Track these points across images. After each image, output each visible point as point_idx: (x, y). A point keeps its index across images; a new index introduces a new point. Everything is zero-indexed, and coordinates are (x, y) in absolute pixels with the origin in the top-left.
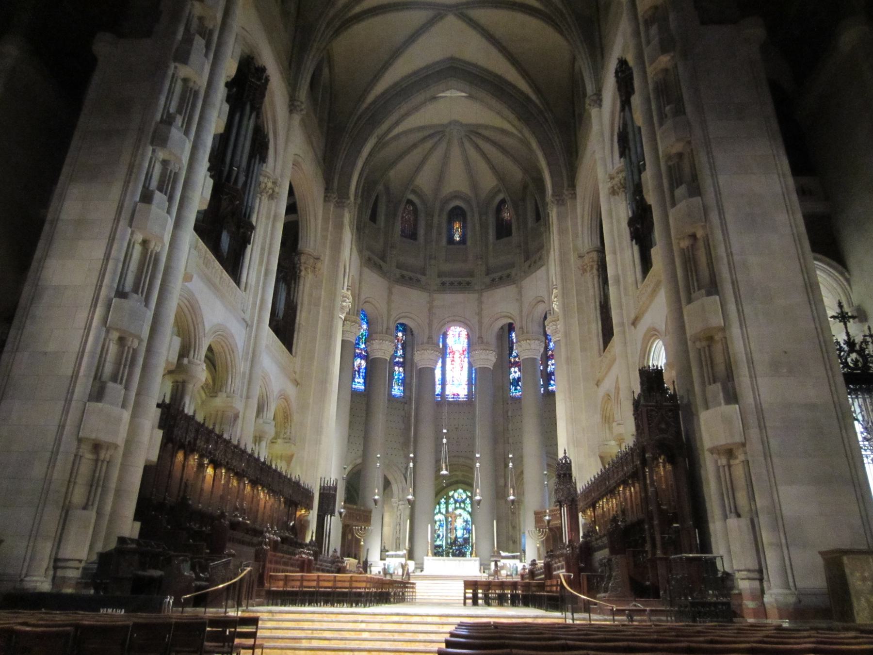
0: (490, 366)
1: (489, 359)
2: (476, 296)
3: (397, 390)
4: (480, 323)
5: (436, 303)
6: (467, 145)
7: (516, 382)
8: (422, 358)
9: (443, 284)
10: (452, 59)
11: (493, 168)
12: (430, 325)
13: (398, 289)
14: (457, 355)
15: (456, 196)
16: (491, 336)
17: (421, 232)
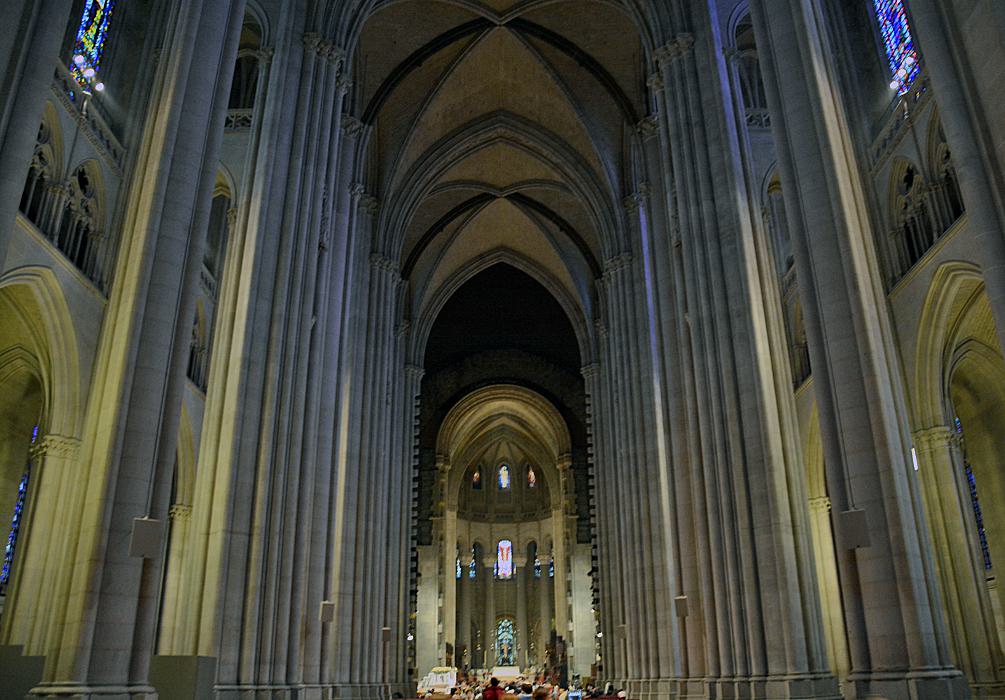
0: (523, 565)
1: (522, 562)
2: (515, 525)
3: (472, 574)
4: (518, 542)
5: (495, 529)
6: (512, 445)
7: (538, 568)
8: (488, 562)
9: (498, 517)
10: (503, 425)
11: (525, 454)
12: (491, 542)
13: (473, 524)
14: (505, 552)
15: (503, 459)
16: (523, 550)
17: (484, 483)
